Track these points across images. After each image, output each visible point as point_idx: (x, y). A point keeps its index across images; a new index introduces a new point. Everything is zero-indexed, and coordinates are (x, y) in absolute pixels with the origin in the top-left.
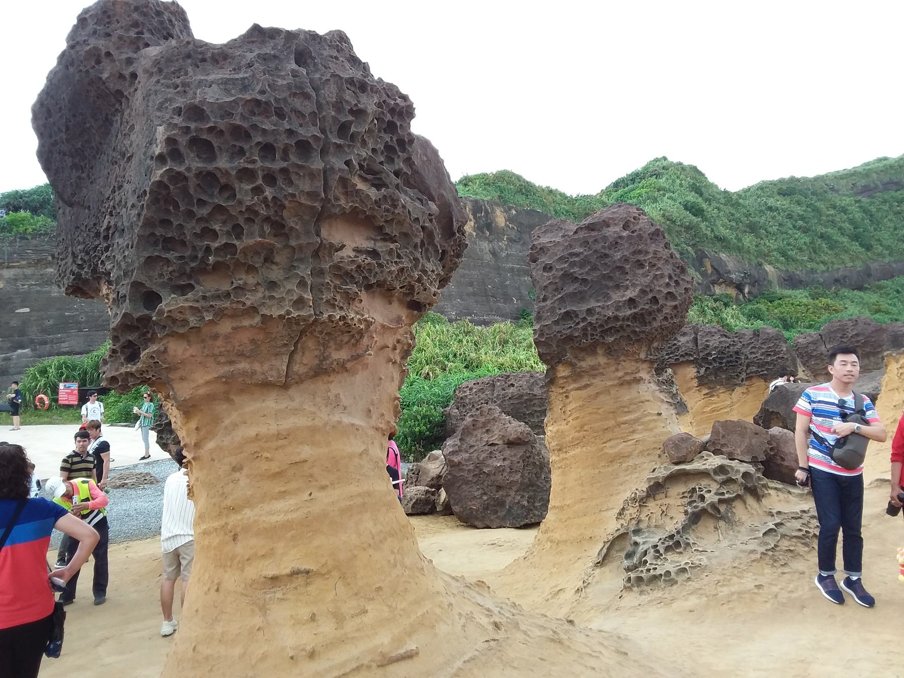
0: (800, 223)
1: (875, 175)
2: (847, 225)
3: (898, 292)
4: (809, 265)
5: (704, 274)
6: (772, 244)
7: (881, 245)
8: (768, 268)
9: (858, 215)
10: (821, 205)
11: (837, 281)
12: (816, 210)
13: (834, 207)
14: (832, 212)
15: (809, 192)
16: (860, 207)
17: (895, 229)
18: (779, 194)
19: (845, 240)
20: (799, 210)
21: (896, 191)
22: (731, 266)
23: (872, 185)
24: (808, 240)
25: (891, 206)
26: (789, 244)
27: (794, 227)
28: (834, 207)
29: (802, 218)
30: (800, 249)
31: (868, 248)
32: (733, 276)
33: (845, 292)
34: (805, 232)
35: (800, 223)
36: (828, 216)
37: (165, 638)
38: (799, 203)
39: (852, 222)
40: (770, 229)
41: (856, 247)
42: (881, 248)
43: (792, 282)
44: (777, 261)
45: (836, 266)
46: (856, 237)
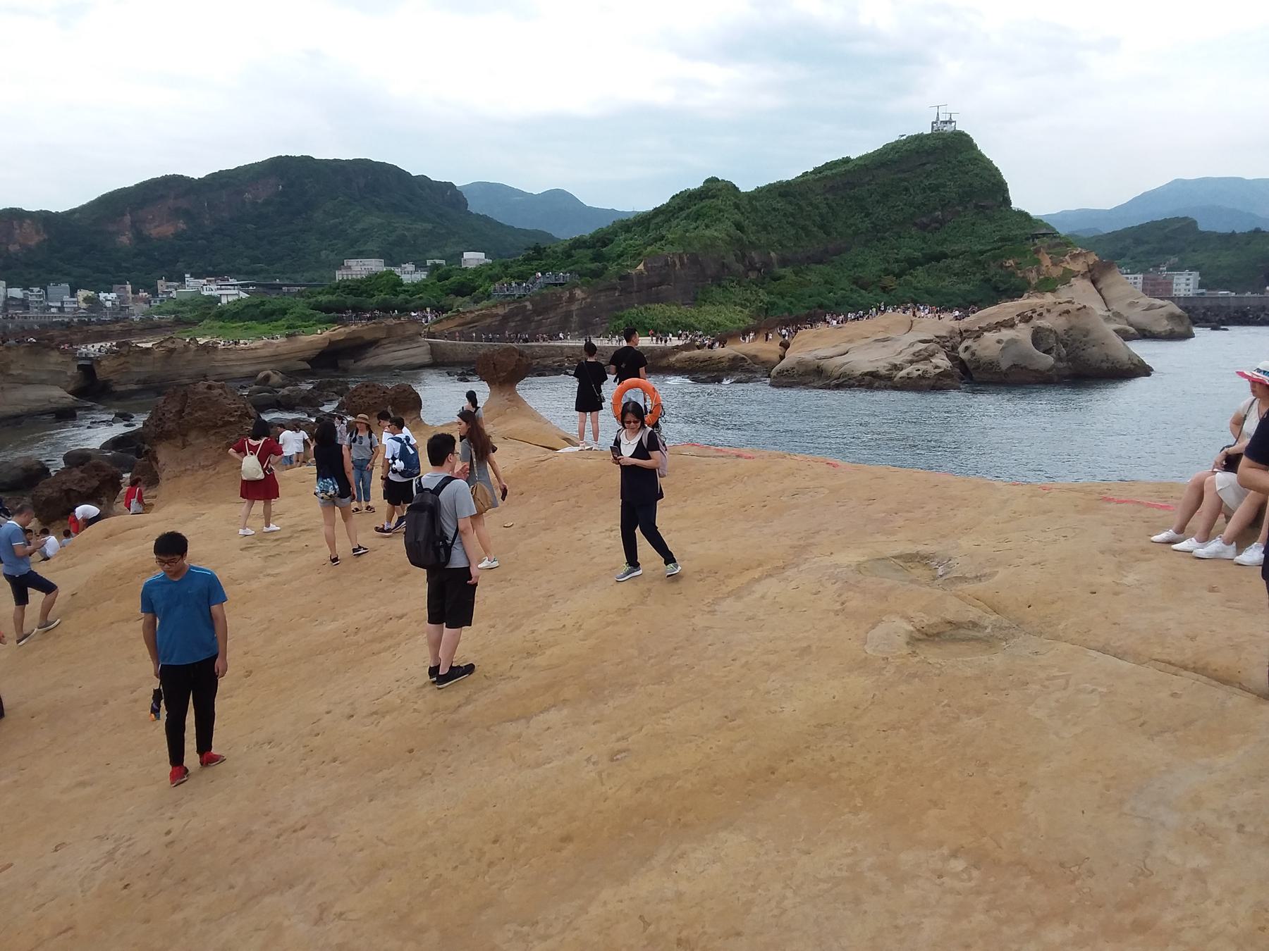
0: (791, 219)
1: (838, 178)
2: (818, 219)
3: (842, 264)
4: (794, 248)
5: (745, 266)
6: (775, 237)
7: (836, 232)
8: (773, 254)
9: (824, 210)
10: (803, 203)
11: (808, 257)
12: (800, 208)
13: (811, 204)
14: (810, 208)
15: (797, 194)
16: (827, 204)
17: (846, 218)
18: (779, 195)
19: (815, 229)
20: (790, 209)
21: (851, 189)
22: (756, 260)
23: (836, 185)
24: (794, 232)
25: (846, 201)
26: (784, 236)
27: (787, 222)
28: (811, 204)
29: (792, 215)
30: (790, 239)
31: (828, 234)
32: (757, 266)
33: (813, 266)
34: (792, 226)
35: (791, 219)
36: (807, 211)
37: (46, 634)
38: (790, 203)
39: (821, 215)
40: (774, 226)
41: (821, 235)
42: (835, 234)
43: (784, 263)
44: (777, 249)
45: (808, 248)
46: (822, 227)
